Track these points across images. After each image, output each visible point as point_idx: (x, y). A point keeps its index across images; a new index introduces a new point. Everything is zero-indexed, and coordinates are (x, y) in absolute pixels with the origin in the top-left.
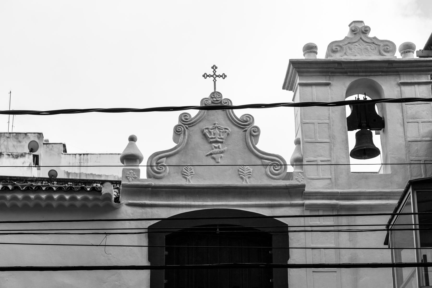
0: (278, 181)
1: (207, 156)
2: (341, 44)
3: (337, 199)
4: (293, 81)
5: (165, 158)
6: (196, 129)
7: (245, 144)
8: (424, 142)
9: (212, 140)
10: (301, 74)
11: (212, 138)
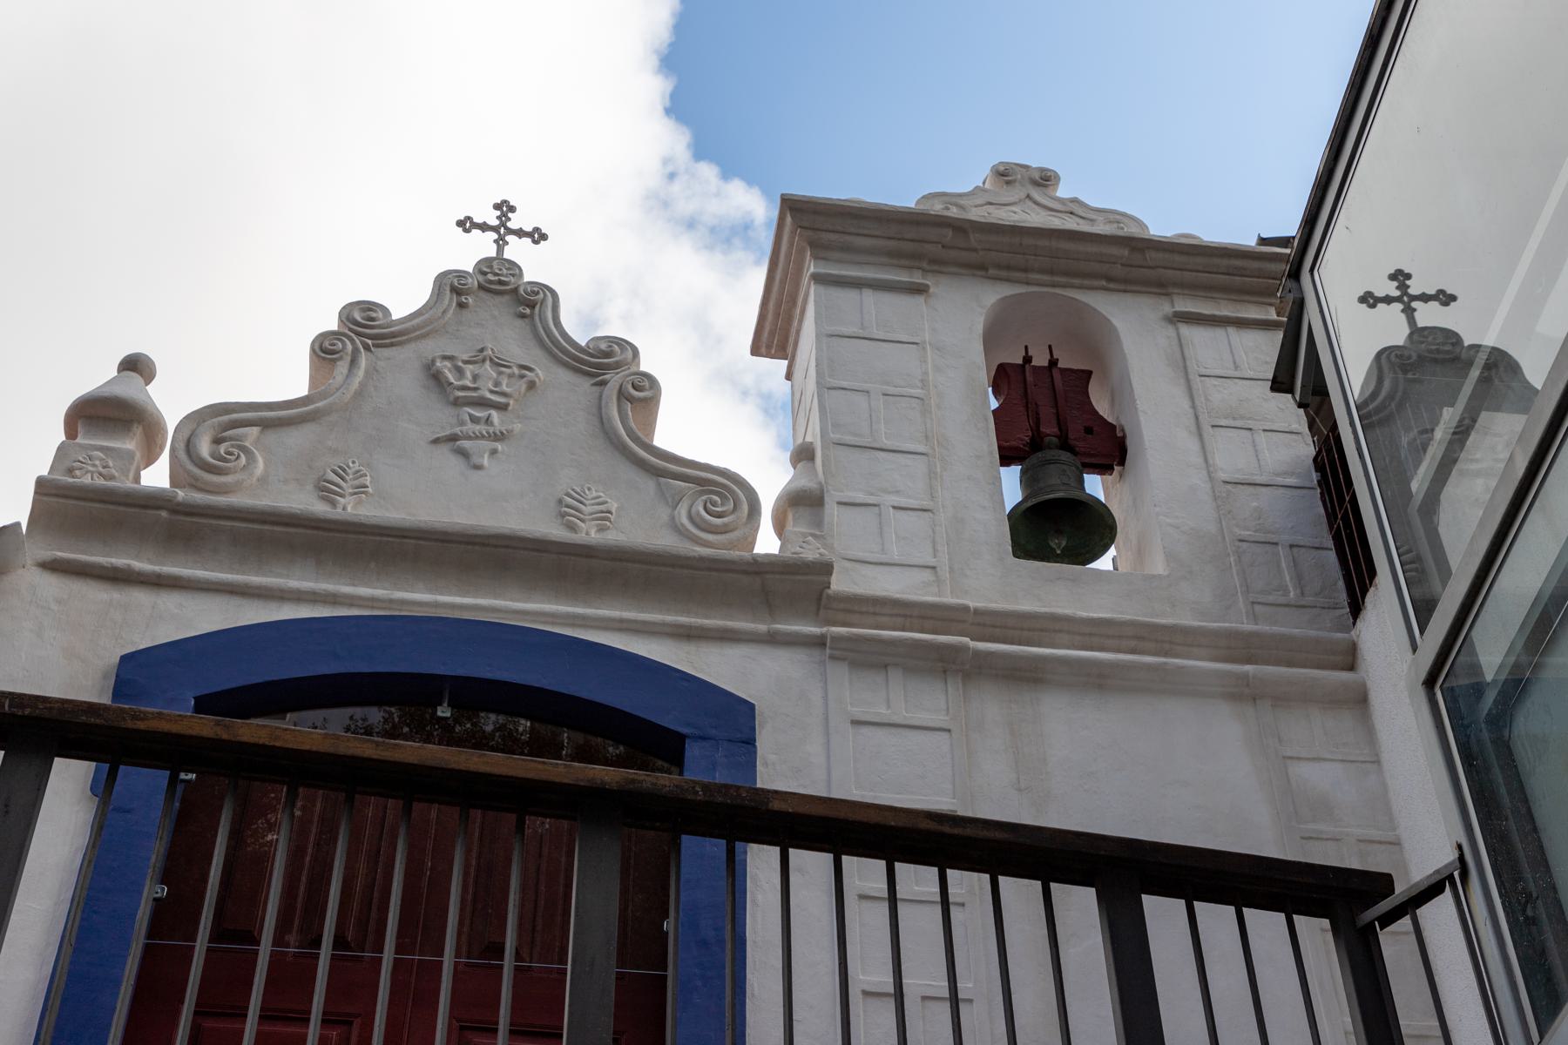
1: (436, 441)
5: (255, 430)
6: (408, 357)
8: (1282, 490)
10: (820, 249)
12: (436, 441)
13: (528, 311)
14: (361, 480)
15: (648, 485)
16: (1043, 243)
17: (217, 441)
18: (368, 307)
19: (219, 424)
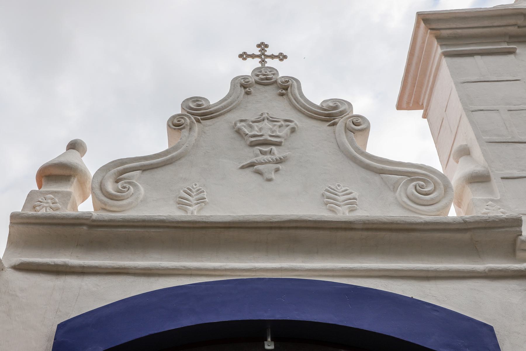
1: (243, 168)
12: (243, 168)
13: (284, 91)
14: (201, 195)
15: (376, 178)
18: (196, 99)
19: (118, 171)
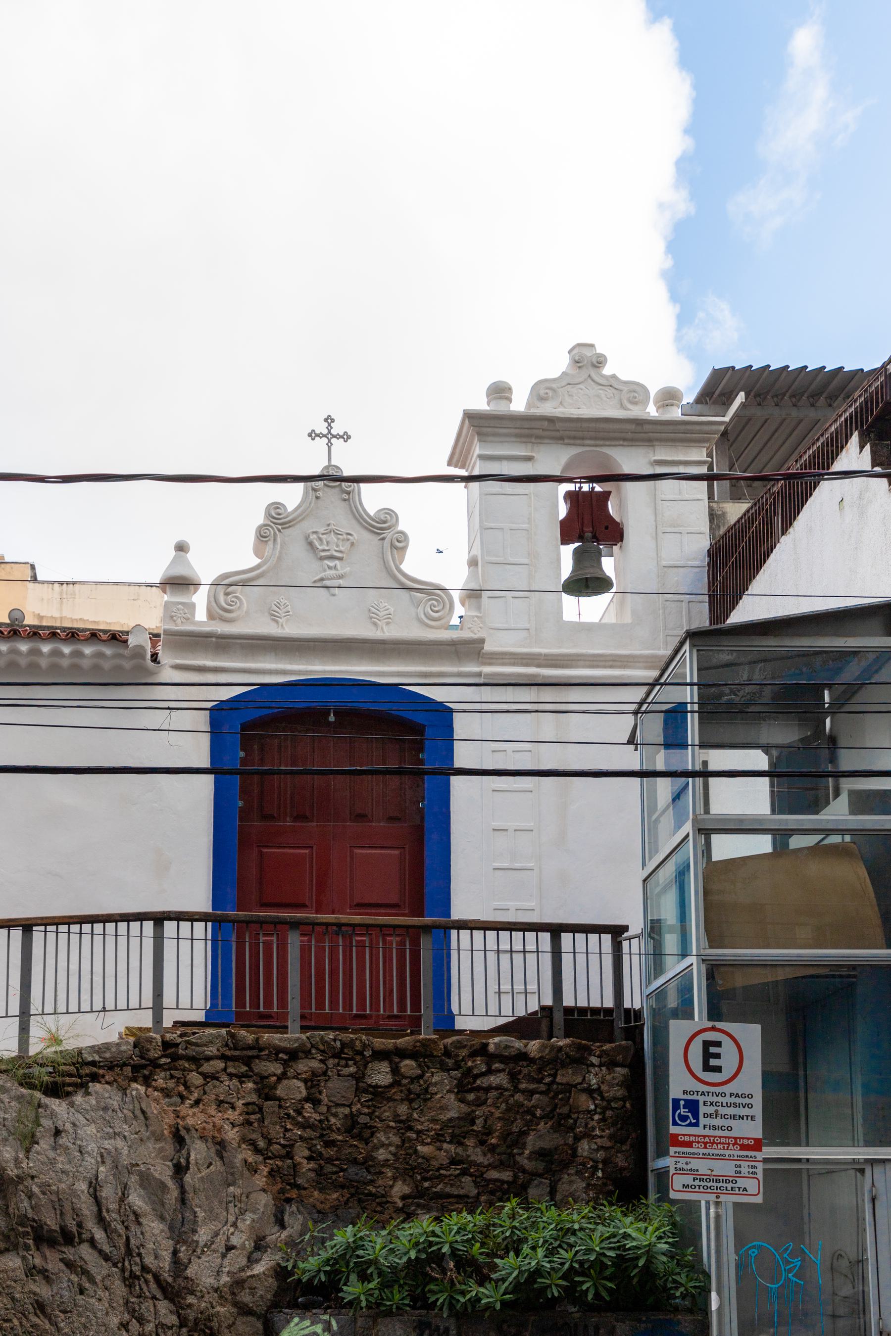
0: (438, 631)
2: (554, 386)
3: (538, 666)
4: (468, 451)
6: (295, 533)
7: (382, 562)
9: (323, 554)
10: (482, 436)
11: (324, 550)
16: (593, 425)
17: (227, 594)
